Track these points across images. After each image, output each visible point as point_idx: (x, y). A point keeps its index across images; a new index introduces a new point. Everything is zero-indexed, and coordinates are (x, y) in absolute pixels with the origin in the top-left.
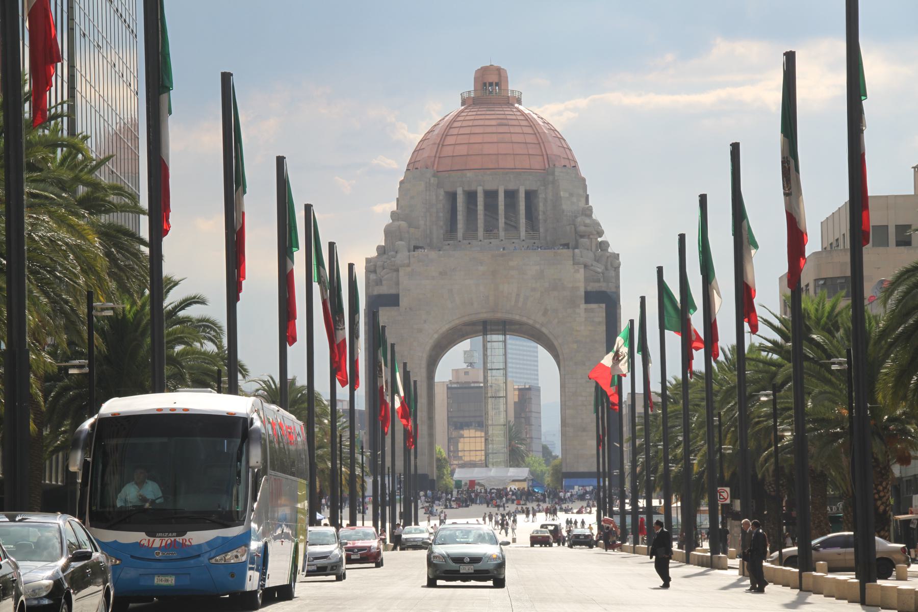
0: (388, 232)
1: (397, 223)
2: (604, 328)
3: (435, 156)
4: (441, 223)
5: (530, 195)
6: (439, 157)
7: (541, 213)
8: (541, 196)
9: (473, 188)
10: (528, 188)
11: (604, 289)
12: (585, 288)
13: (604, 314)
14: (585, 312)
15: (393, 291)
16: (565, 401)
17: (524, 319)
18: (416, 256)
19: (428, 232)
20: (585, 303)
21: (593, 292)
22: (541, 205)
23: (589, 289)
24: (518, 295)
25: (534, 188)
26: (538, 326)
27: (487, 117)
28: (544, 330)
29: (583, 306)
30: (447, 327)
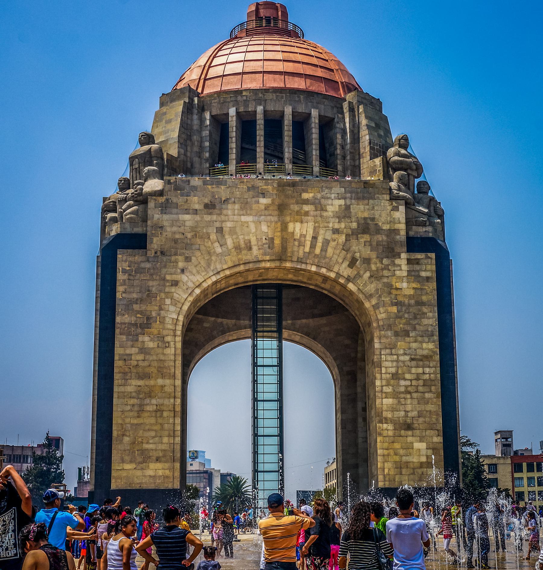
1: (146, 147)
3: (200, 79)
4: (207, 155)
6: (205, 80)
7: (339, 147)
11: (431, 235)
12: (407, 233)
13: (434, 267)
14: (408, 264)
15: (138, 230)
16: (382, 386)
17: (324, 271)
18: (172, 181)
19: (189, 165)
21: (417, 238)
22: (339, 136)
23: (411, 234)
24: (315, 238)
26: (342, 281)
27: (266, 42)
28: (351, 286)
29: (404, 256)
30: (214, 279)
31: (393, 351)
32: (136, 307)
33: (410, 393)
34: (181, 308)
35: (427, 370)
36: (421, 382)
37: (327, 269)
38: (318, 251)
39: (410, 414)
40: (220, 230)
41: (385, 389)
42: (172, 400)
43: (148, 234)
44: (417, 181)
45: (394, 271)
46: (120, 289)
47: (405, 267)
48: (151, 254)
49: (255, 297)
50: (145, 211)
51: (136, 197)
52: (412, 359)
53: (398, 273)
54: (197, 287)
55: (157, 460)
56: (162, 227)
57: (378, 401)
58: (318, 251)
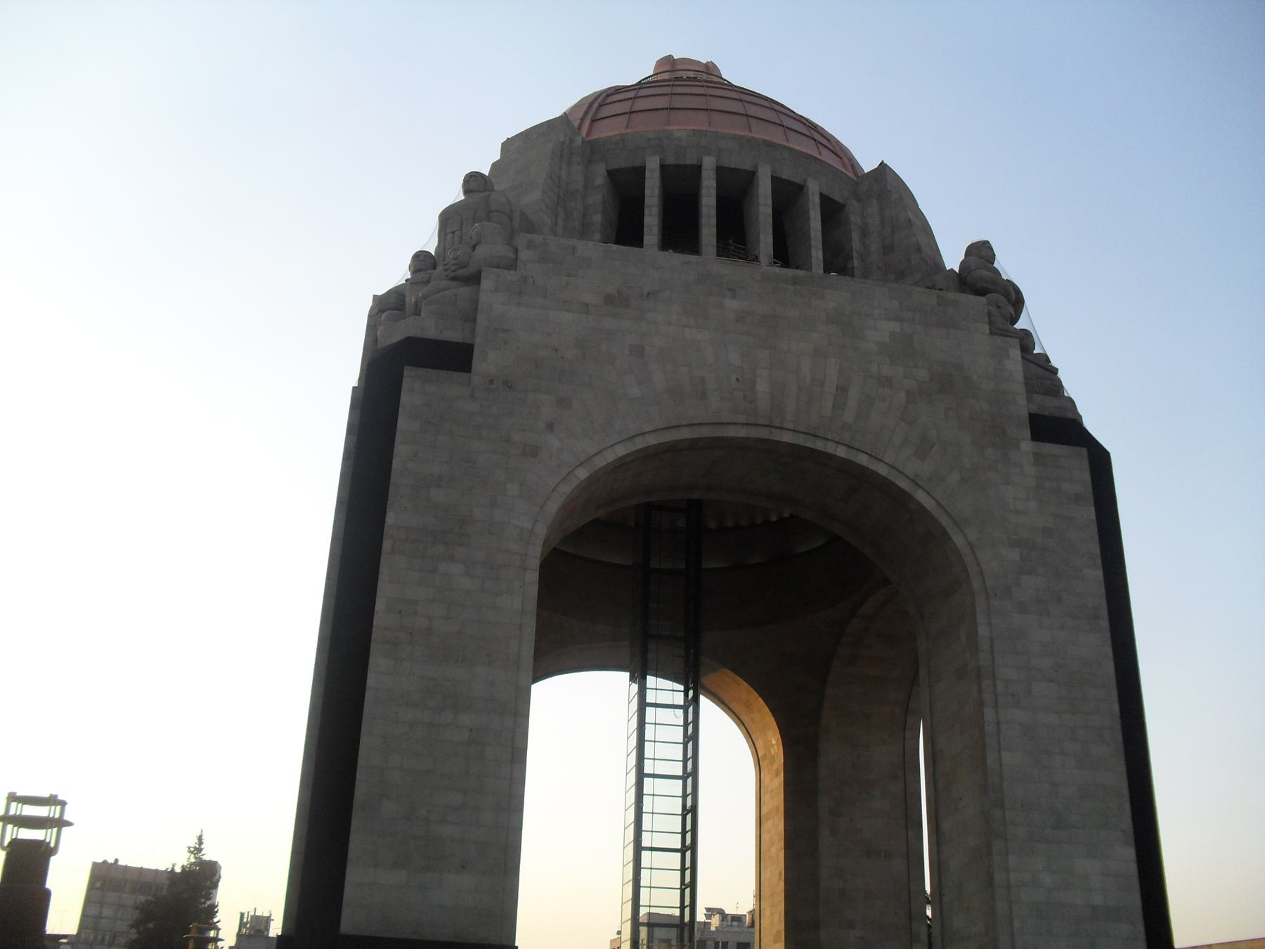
0: (450, 219)
3: (582, 120)
5: (832, 211)
6: (593, 121)
7: (855, 255)
8: (855, 219)
9: (690, 160)
10: (825, 192)
13: (1087, 476)
15: (454, 335)
17: (863, 459)
22: (855, 237)
23: (1034, 409)
24: (842, 390)
25: (837, 198)
26: (903, 484)
28: (921, 496)
29: (1027, 446)
30: (621, 451)
34: (542, 508)
37: (870, 455)
38: (849, 416)
40: (638, 351)
43: (479, 343)
46: (401, 451)
50: (475, 302)
51: (454, 271)
54: (581, 464)
55: (463, 867)
57: (991, 758)
58: (849, 416)
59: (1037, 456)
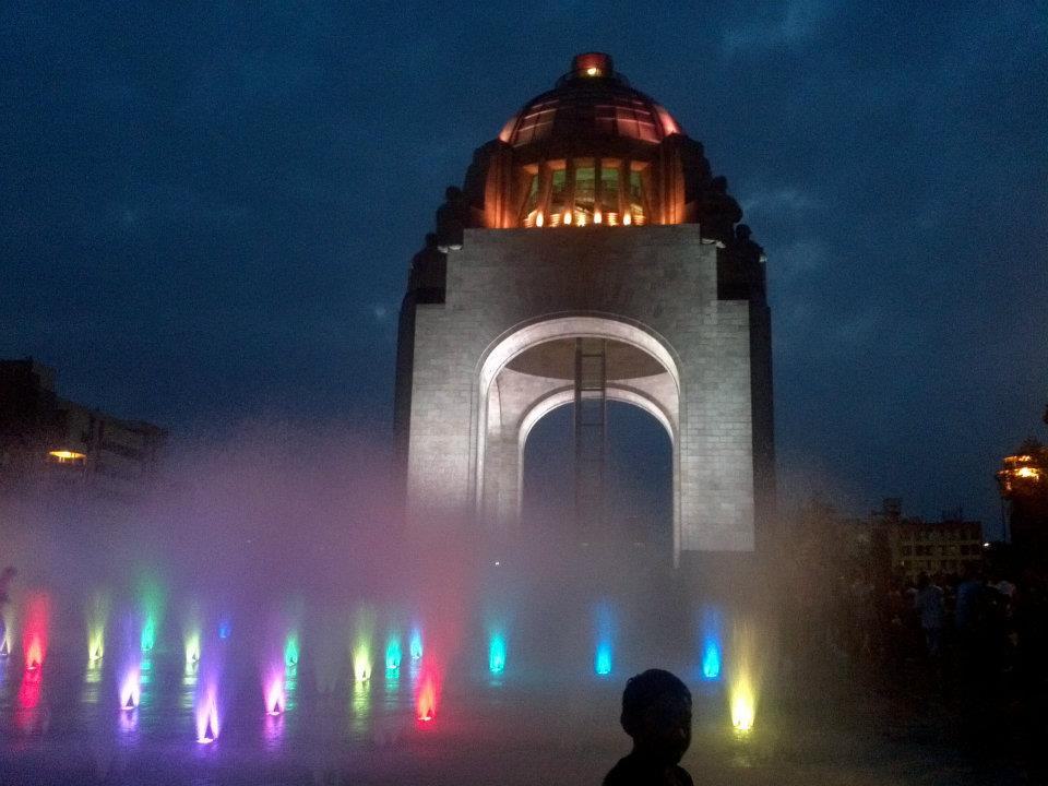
2: (748, 334)
13: (747, 315)
20: (720, 297)
29: (715, 303)
31: (701, 405)
32: (433, 362)
33: (717, 450)
35: (738, 425)
36: (730, 439)
39: (718, 474)
41: (691, 446)
42: (467, 457)
44: (736, 225)
45: (703, 320)
47: (714, 316)
48: (447, 306)
49: (579, 355)
52: (721, 414)
53: (707, 322)
56: (461, 280)
59: (720, 310)
